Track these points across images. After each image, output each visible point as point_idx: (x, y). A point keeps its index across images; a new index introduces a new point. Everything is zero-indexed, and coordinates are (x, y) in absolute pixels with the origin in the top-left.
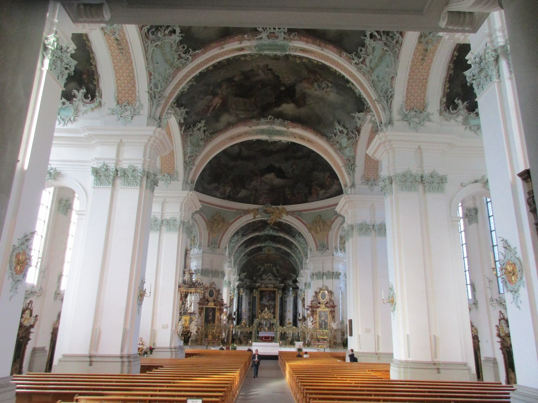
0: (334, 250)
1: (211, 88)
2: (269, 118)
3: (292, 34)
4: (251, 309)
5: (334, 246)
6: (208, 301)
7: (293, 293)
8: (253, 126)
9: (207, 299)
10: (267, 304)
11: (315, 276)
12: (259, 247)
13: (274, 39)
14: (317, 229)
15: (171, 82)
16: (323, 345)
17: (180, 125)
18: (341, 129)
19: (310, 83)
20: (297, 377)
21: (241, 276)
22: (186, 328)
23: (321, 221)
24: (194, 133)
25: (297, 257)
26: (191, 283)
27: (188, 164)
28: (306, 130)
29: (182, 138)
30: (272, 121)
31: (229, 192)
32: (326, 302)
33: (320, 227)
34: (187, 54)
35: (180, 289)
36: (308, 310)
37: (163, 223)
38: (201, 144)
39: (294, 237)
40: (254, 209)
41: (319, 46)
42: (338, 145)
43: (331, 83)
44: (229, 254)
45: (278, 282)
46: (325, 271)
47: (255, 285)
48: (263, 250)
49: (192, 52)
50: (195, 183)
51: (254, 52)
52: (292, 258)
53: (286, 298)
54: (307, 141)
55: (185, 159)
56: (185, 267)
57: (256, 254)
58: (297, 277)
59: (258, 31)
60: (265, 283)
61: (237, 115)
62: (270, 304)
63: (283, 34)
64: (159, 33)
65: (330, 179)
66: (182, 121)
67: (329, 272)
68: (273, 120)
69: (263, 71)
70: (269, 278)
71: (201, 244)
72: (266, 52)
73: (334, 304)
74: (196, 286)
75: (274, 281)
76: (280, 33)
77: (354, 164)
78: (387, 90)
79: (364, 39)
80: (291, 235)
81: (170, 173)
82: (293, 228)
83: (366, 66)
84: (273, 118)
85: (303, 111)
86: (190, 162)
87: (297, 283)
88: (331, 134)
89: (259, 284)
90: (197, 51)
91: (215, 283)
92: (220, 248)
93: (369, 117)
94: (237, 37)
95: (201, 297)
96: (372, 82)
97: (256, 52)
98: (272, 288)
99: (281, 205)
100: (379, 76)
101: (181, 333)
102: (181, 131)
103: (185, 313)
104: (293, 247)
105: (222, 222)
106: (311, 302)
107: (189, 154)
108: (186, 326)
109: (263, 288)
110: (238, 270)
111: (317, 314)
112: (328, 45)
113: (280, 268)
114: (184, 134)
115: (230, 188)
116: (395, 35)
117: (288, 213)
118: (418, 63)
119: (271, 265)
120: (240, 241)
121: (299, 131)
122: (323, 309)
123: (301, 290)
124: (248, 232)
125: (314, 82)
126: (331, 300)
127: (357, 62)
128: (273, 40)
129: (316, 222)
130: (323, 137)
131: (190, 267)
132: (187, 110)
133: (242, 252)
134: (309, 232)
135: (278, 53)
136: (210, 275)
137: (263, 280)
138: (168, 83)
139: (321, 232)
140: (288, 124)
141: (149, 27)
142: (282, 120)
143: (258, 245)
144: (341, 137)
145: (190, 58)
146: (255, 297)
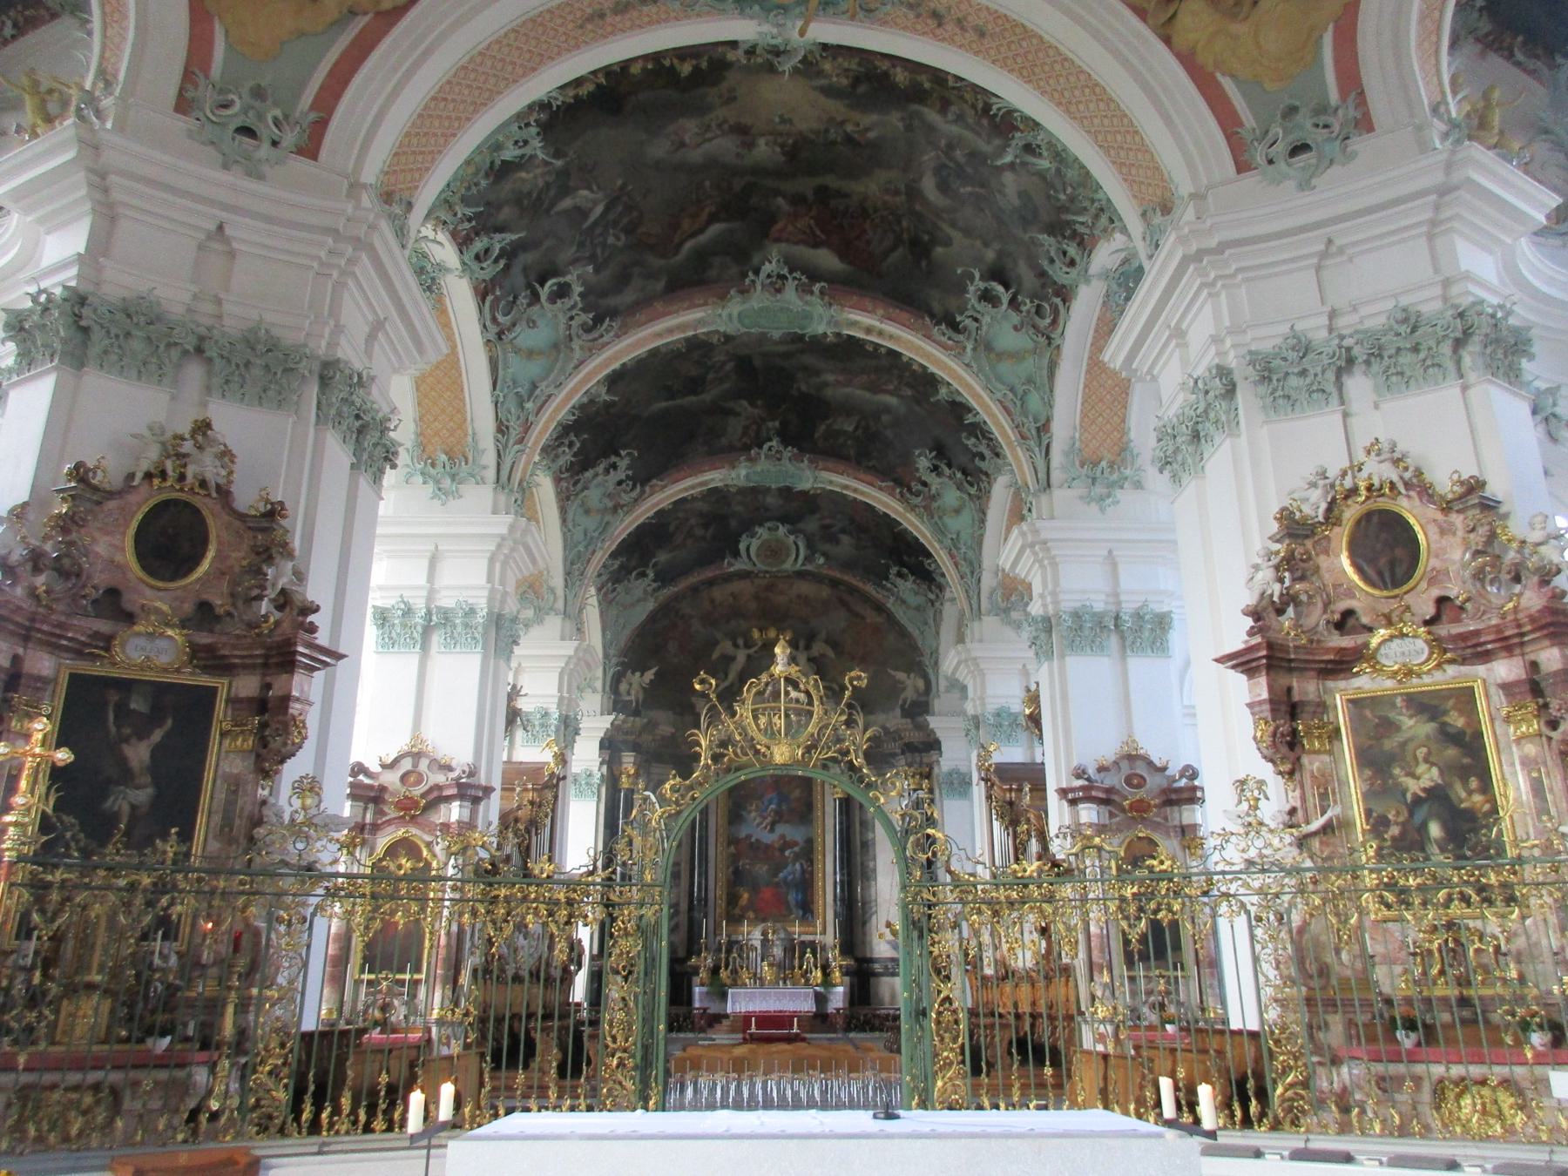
6: (113, 604)
9: (113, 593)
10: (768, 838)
11: (1245, 398)
12: (717, 495)
16: (1506, 1083)
21: (623, 687)
25: (940, 531)
44: (502, 429)
48: (742, 547)
52: (899, 581)
57: (708, 573)
62: (783, 837)
67: (1411, 321)
80: (932, 316)
87: (929, 718)
104: (923, 463)
110: (606, 656)
113: (831, 653)
120: (578, 354)
124: (628, 297)
143: (715, 477)
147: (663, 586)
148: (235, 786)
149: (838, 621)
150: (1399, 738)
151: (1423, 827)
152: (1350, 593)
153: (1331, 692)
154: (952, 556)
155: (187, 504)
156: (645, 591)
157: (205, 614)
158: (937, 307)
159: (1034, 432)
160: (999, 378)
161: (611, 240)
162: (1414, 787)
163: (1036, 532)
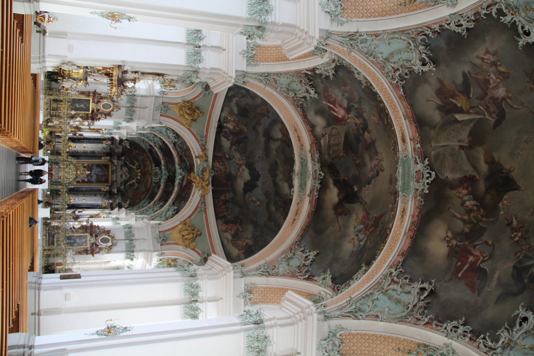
1: (356, 106)
3: (422, 198)
13: (416, 178)
34: (399, 78)
41: (409, 230)
49: (401, 84)
51: (401, 155)
59: (425, 160)
63: (422, 187)
64: (423, 47)
68: (319, 178)
69: (376, 166)
72: (400, 169)
76: (423, 185)
78: (364, 312)
79: (419, 282)
83: (389, 285)
85: (329, 212)
90: (402, 90)
93: (329, 292)
94: (417, 136)
96: (371, 293)
97: (400, 157)
100: (379, 300)
112: (410, 240)
116: (426, 317)
118: (394, 345)
121: (306, 208)
127: (393, 275)
128: (414, 176)
135: (400, 183)
141: (430, 35)
145: (395, 82)
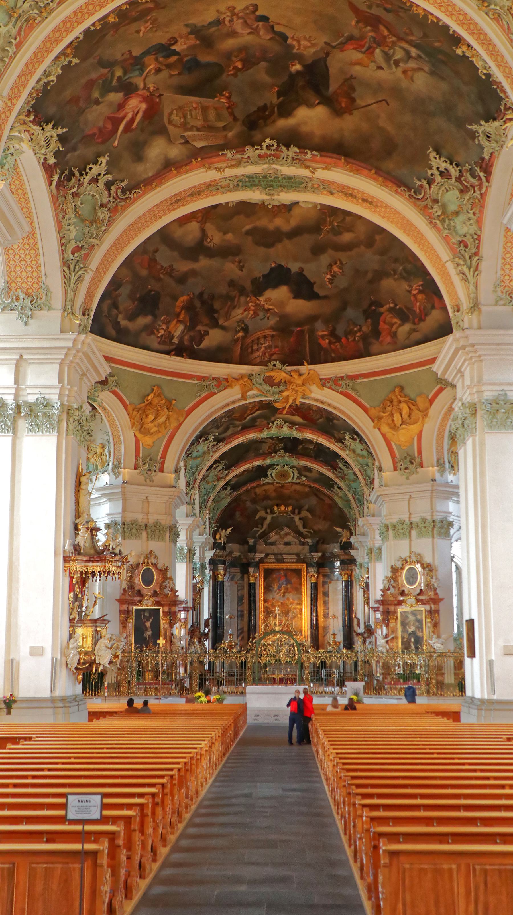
0: (436, 468)
2: (264, 145)
4: (246, 612)
5: (435, 460)
6: (139, 593)
7: (343, 573)
8: (228, 167)
9: (139, 591)
11: (391, 532)
12: (259, 467)
14: (395, 419)
15: (12, 58)
17: (48, 170)
18: (443, 166)
19: (363, 50)
20: (337, 753)
21: (218, 537)
22: (86, 653)
23: (402, 399)
24: (82, 190)
25: (349, 487)
26: (92, 552)
27: (72, 268)
28: (357, 172)
29: (54, 204)
30: (273, 153)
31: (181, 339)
32: (418, 591)
33: (401, 415)
35: (67, 565)
36: (378, 611)
37: (19, 412)
38: (102, 217)
39: (340, 440)
40: (242, 377)
42: (436, 206)
43: (416, 46)
44: (187, 485)
45: (307, 548)
46: (415, 519)
47: (253, 558)
48: (269, 474)
50: (92, 314)
52: (338, 490)
53: (326, 586)
54: (360, 201)
55: (65, 256)
56: (78, 515)
57: (253, 485)
58: (351, 534)
60: (276, 551)
61: (187, 142)
65: (424, 296)
66: (52, 161)
67: (424, 520)
70: (286, 540)
71: (119, 462)
73: (436, 594)
74: (105, 556)
75: (296, 548)
77: (476, 254)
80: (335, 438)
81: (30, 291)
82: (339, 418)
84: (275, 145)
86: (78, 261)
87: (351, 551)
88: (420, 181)
89: (262, 555)
91: (156, 552)
92: (165, 470)
95: (125, 586)
98: (292, 563)
99: (305, 363)
101: (75, 665)
102: (50, 184)
103: (80, 620)
104: (341, 465)
105: (166, 410)
106: (382, 591)
107: (73, 242)
108: (86, 649)
109: (272, 563)
111: (397, 618)
113: (310, 516)
114: (58, 193)
115: (181, 327)
117: (324, 383)
119: (290, 509)
120: (211, 453)
122: (412, 606)
123: (361, 566)
124: (229, 432)
125: (375, 45)
126: (428, 585)
129: (391, 402)
130: (399, 190)
131: (89, 515)
132: (60, 131)
133: (219, 479)
134: (374, 427)
136: (144, 534)
137: (272, 544)
138: (7, 60)
139: (403, 426)
140: (313, 160)
142: (298, 151)
144: (443, 188)
146: (254, 584)
147: (234, 491)
148: (166, 630)
149: (313, 501)
150: (409, 620)
151: (410, 639)
152: (404, 586)
153: (397, 609)
154: (354, 498)
155: (148, 569)
156: (226, 494)
157: (155, 594)
158: (336, 435)
159: (369, 483)
160: (358, 461)
161: (223, 420)
162: (410, 630)
163: (357, 538)
